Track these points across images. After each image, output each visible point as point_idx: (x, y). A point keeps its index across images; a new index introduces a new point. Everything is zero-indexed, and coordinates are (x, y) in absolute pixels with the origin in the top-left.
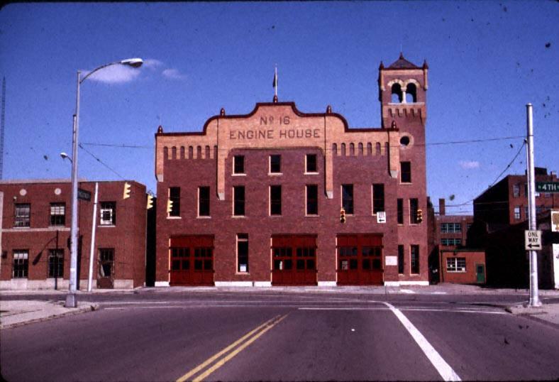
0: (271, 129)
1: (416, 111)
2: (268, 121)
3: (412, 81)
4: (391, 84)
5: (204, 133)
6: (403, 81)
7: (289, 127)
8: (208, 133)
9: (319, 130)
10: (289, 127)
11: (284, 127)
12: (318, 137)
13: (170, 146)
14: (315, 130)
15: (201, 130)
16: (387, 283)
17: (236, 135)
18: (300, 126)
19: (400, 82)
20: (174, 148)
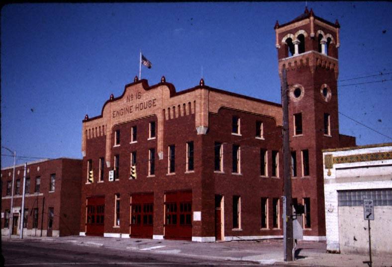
0: (131, 105)
1: (305, 61)
2: (131, 99)
3: (302, 32)
4: (284, 40)
5: (101, 116)
6: (294, 34)
7: (141, 101)
8: (104, 116)
9: (155, 99)
10: (141, 101)
11: (138, 102)
12: (155, 105)
13: (88, 129)
14: (153, 100)
15: (100, 114)
16: (194, 239)
17: (116, 113)
18: (146, 99)
19: (292, 36)
20: (90, 130)
